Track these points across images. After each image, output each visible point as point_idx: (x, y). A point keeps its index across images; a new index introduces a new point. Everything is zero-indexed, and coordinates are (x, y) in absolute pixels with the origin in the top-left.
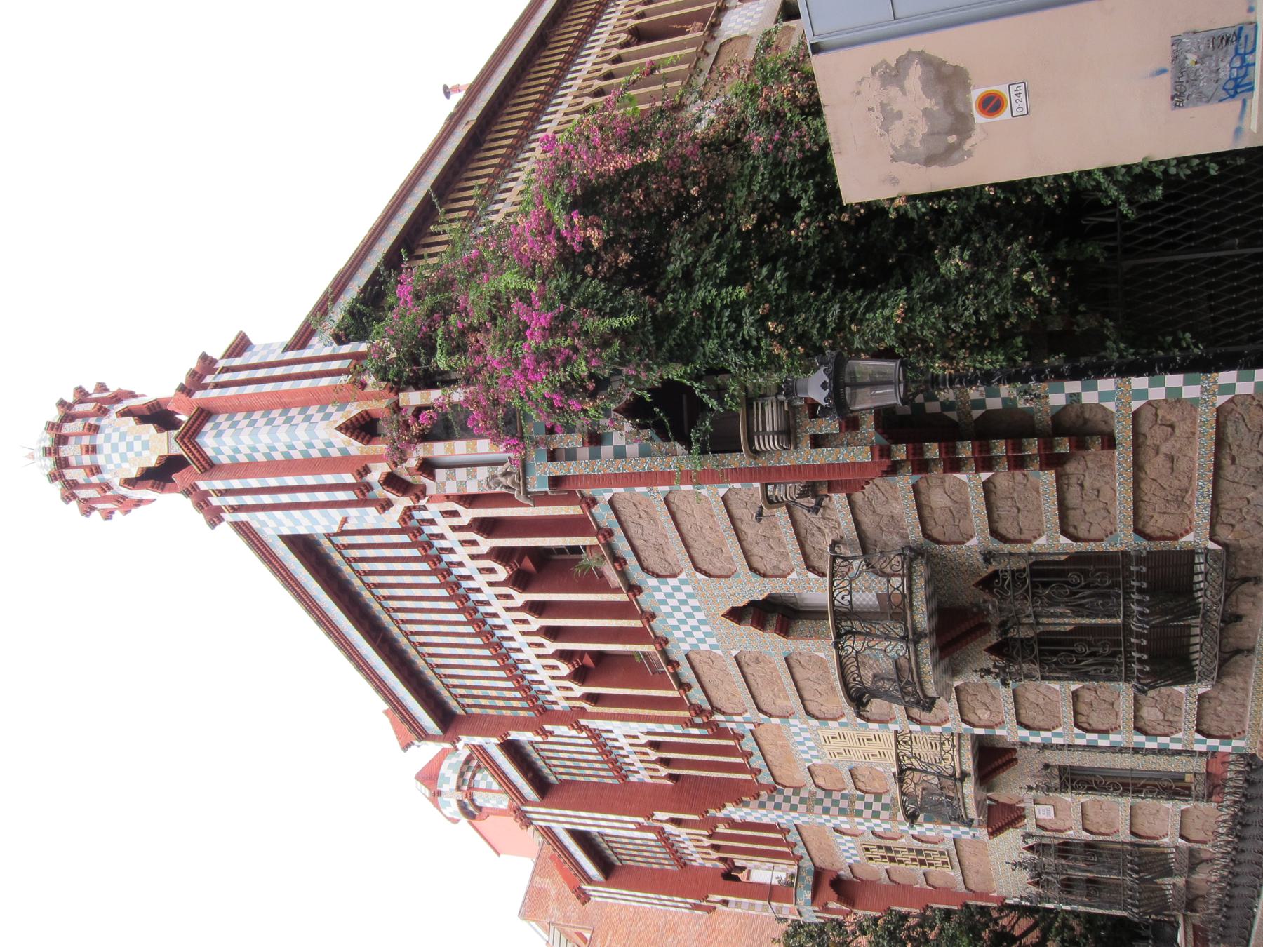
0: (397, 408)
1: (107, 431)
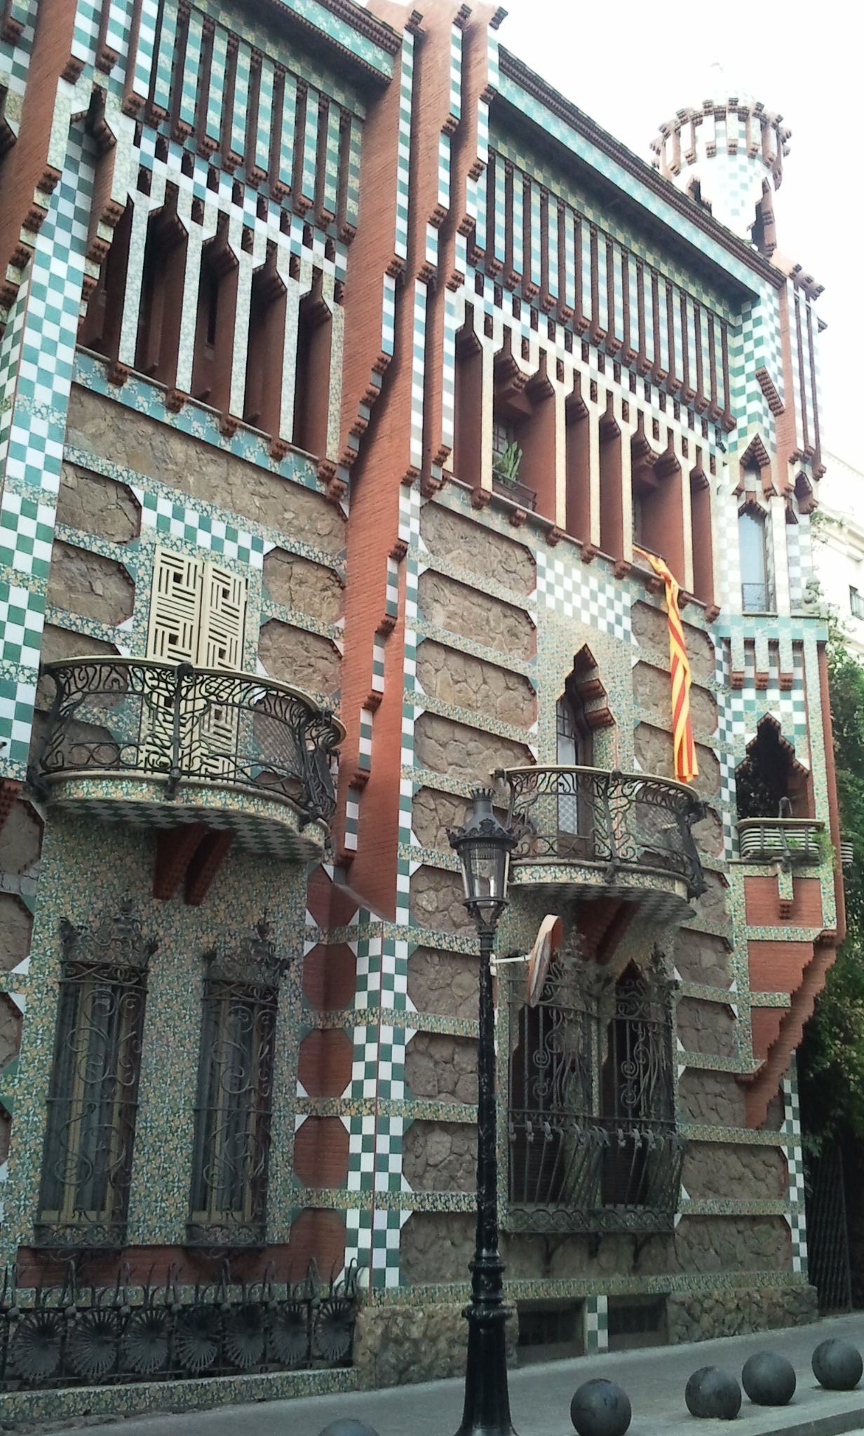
0: (769, 493)
1: (750, 168)
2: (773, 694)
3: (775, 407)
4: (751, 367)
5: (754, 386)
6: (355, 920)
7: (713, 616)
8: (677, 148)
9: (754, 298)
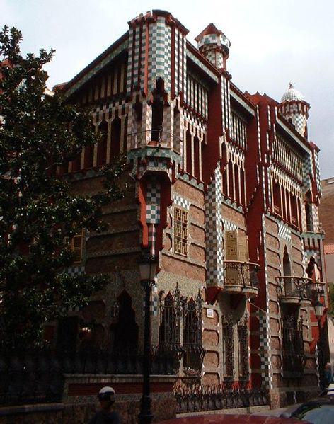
0: (311, 202)
2: (313, 251)
3: (312, 181)
4: (307, 172)
5: (309, 176)
6: (258, 312)
7: (301, 232)
8: (286, 110)
9: (309, 155)
